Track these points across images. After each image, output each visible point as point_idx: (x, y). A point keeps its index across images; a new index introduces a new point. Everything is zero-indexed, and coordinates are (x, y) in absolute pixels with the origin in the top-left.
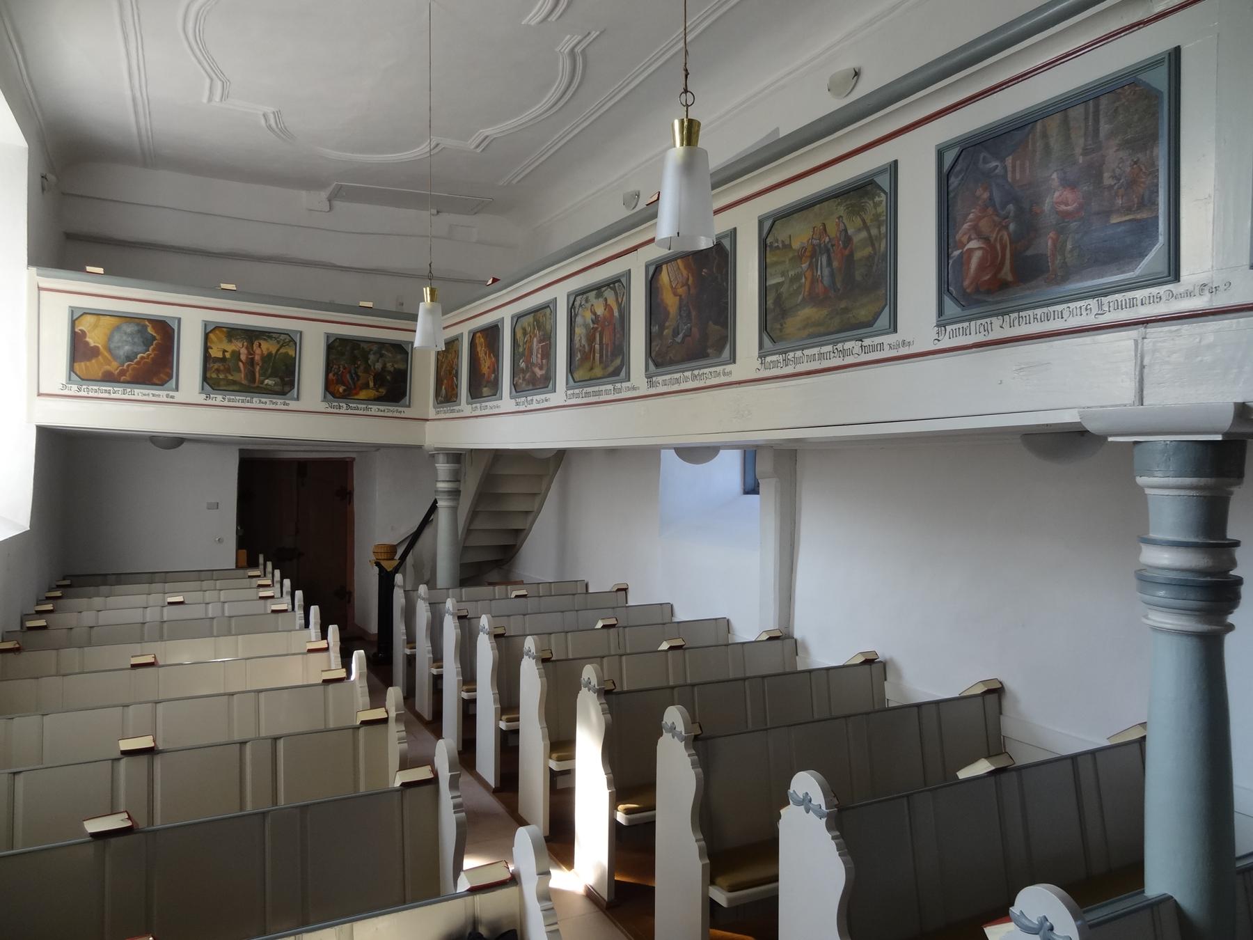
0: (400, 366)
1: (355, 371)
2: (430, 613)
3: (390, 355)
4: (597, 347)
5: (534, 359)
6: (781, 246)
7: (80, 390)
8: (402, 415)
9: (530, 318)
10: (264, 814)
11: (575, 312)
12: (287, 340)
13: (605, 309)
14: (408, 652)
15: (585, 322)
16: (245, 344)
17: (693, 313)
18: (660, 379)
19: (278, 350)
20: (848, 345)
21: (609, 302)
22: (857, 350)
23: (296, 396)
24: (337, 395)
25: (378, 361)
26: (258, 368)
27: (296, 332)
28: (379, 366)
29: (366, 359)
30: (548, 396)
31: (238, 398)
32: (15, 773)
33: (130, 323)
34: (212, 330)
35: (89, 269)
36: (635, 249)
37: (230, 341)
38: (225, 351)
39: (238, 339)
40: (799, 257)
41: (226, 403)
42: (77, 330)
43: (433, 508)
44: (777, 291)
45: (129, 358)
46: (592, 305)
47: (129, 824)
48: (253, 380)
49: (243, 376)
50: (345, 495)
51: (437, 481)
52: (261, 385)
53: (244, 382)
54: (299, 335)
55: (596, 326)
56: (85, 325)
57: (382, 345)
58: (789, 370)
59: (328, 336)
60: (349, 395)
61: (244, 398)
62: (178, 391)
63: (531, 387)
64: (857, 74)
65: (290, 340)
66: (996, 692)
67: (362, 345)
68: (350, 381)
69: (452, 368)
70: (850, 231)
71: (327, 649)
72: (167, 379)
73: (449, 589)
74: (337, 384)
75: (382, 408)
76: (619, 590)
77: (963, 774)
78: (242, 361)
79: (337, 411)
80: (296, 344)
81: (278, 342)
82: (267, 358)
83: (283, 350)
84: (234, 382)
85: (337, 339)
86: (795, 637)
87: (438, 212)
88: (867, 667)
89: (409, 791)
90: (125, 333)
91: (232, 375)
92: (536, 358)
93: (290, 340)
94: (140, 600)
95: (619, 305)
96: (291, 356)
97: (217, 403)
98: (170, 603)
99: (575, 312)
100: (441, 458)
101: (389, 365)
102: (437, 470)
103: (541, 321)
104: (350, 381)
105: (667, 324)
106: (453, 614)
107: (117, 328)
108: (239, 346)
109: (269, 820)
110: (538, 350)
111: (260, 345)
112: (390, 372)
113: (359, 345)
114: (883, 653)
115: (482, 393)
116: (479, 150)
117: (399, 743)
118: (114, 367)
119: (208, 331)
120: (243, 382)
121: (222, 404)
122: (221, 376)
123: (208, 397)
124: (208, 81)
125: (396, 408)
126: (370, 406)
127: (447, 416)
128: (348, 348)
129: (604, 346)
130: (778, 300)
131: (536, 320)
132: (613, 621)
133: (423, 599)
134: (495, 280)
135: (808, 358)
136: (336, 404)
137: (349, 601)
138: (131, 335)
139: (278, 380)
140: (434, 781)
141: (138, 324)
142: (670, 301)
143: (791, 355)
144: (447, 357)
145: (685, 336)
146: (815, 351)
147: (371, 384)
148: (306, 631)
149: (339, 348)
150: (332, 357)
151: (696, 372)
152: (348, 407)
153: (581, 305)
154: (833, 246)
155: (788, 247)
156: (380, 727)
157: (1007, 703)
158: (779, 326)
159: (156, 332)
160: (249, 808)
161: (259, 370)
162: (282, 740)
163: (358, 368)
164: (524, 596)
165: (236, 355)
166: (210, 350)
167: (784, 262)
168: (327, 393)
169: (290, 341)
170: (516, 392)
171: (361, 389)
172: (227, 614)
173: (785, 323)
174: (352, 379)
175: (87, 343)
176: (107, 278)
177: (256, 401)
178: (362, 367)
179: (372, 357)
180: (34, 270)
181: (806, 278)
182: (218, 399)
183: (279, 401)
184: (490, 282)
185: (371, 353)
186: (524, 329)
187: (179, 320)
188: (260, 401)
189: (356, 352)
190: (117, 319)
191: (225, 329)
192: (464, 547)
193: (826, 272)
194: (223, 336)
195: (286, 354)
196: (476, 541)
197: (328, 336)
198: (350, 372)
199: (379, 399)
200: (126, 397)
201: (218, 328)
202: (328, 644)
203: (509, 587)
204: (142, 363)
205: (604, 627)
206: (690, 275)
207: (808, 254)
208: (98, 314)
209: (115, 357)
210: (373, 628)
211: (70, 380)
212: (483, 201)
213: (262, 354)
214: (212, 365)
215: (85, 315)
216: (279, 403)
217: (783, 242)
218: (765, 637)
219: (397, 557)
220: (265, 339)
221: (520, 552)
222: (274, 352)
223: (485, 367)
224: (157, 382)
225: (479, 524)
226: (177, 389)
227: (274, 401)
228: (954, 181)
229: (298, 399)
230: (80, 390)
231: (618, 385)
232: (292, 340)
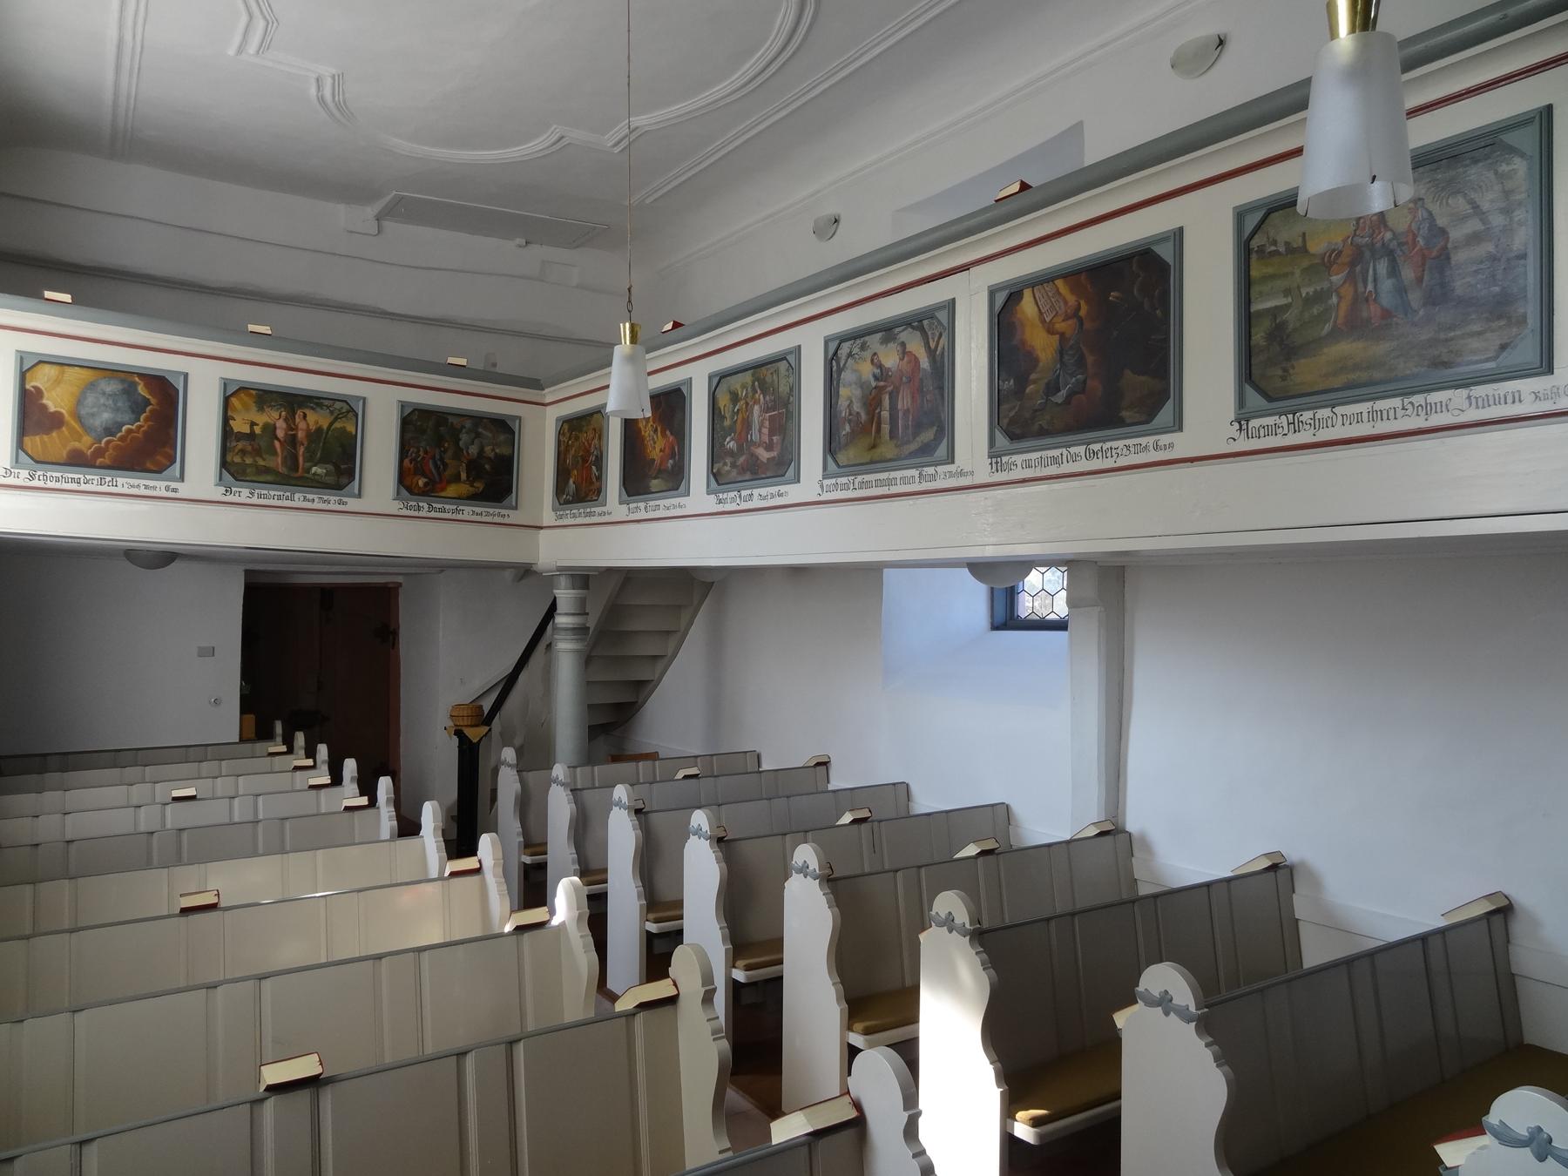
0: (504, 451)
1: (441, 456)
3: (490, 435)
4: (885, 414)
5: (755, 437)
6: (1282, 249)
7: (32, 477)
8: (506, 521)
9: (747, 377)
11: (838, 364)
12: (344, 411)
13: (902, 359)
15: (860, 378)
16: (283, 413)
17: (1090, 359)
18: (1018, 459)
19: (331, 424)
21: (909, 348)
23: (356, 491)
25: (473, 443)
26: (301, 450)
27: (358, 398)
28: (473, 450)
30: (783, 488)
31: (272, 493)
32: (82, 1143)
33: (110, 378)
35: (48, 294)
36: (965, 268)
37: (261, 409)
38: (253, 424)
39: (271, 406)
41: (255, 500)
42: (28, 387)
44: (1275, 318)
45: (109, 431)
46: (875, 354)
48: (295, 467)
50: (387, 635)
52: (306, 475)
54: (361, 403)
55: (882, 384)
57: (478, 420)
59: (403, 405)
60: (433, 490)
61: (282, 493)
62: (183, 481)
63: (747, 477)
64: (1221, 42)
65: (348, 409)
66: (1503, 912)
67: (451, 419)
68: (433, 470)
69: (588, 452)
72: (168, 464)
74: (415, 474)
75: (478, 510)
76: (818, 764)
78: (279, 441)
79: (416, 514)
81: (332, 412)
82: (316, 435)
83: (337, 425)
84: (267, 470)
85: (415, 410)
86: (1132, 826)
88: (1272, 874)
90: (104, 393)
91: (264, 460)
92: (759, 431)
93: (348, 409)
95: (931, 353)
96: (351, 433)
97: (242, 500)
99: (838, 364)
100: (563, 581)
101: (488, 449)
103: (768, 379)
104: (433, 470)
105: (1033, 376)
107: (91, 386)
108: (273, 416)
110: (761, 425)
111: (305, 416)
112: (490, 458)
114: (1292, 855)
115: (648, 487)
116: (617, 150)
117: (714, 1040)
118: (85, 443)
119: (228, 394)
120: (280, 470)
122: (249, 461)
123: (228, 491)
124: (244, 19)
125: (497, 511)
126: (461, 508)
127: (579, 521)
129: (900, 414)
130: (1278, 333)
131: (756, 378)
134: (676, 325)
136: (414, 503)
138: (112, 396)
139: (330, 467)
141: (123, 381)
144: (577, 438)
146: (1364, 407)
147: (464, 476)
149: (419, 423)
151: (1096, 447)
153: (850, 355)
154: (1400, 244)
156: (665, 1011)
157: (1518, 928)
158: (1280, 372)
159: (150, 394)
161: (304, 452)
162: (521, 1044)
163: (445, 452)
164: (695, 776)
165: (270, 429)
166: (231, 422)
167: (1293, 274)
169: (348, 412)
170: (719, 484)
171: (449, 482)
173: (1293, 367)
175: (45, 407)
176: (76, 309)
177: (299, 499)
178: (450, 453)
179: (464, 437)
181: (1340, 298)
182: (243, 494)
184: (669, 326)
185: (464, 431)
187: (186, 376)
188: (305, 497)
189: (442, 428)
191: (254, 392)
193: (1387, 285)
194: (250, 402)
195: (343, 430)
197: (403, 405)
198: (433, 458)
199: (475, 498)
200: (104, 489)
201: (244, 389)
202: (480, 861)
204: (130, 437)
205: (855, 821)
206: (1082, 303)
207: (1344, 259)
209: (87, 429)
211: (17, 462)
212: (595, 228)
214: (234, 444)
215: (40, 366)
216: (333, 501)
217: (1287, 244)
218: (1093, 831)
220: (313, 409)
222: (325, 427)
226: (182, 478)
227: (325, 498)
229: (359, 496)
230: (32, 477)
231: (930, 470)
232: (352, 410)
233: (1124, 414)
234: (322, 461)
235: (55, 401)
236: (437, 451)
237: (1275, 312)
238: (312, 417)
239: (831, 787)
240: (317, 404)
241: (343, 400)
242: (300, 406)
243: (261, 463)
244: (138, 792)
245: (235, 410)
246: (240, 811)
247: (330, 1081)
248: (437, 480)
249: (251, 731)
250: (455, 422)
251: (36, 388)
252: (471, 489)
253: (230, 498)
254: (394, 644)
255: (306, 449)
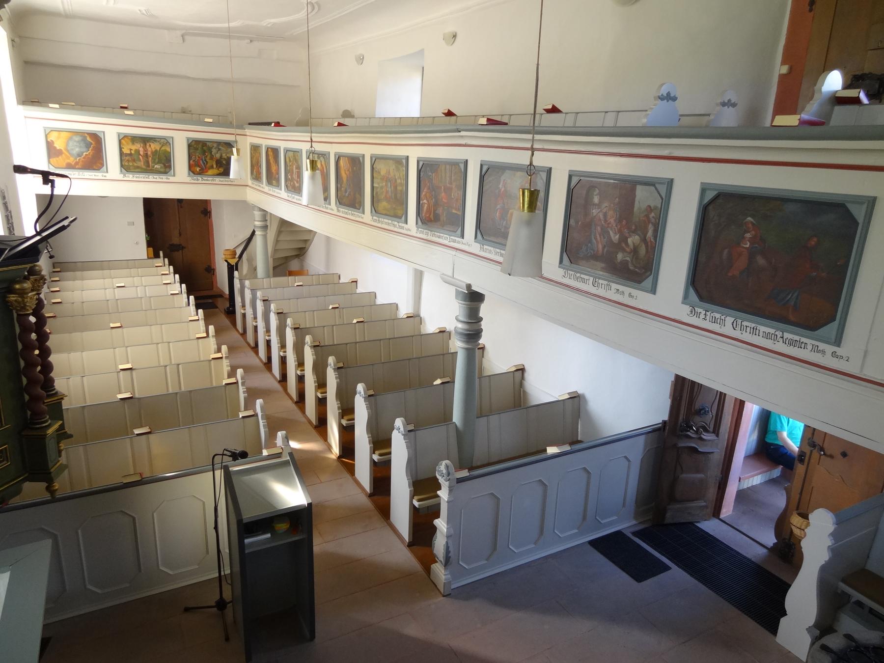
2: (251, 295)
3: (224, 149)
10: (177, 393)
14: (243, 312)
17: (351, 185)
18: (341, 209)
19: (160, 148)
20: (396, 223)
22: (397, 226)
23: (173, 174)
24: (196, 173)
25: (217, 153)
26: (150, 159)
28: (218, 156)
29: (211, 152)
31: (141, 176)
34: (123, 137)
35: (51, 105)
38: (131, 150)
40: (382, 179)
41: (135, 179)
42: (49, 140)
43: (253, 233)
45: (79, 155)
47: (132, 396)
48: (148, 166)
49: (142, 163)
51: (255, 221)
53: (144, 167)
54: (171, 139)
56: (53, 137)
57: (219, 143)
58: (379, 225)
59: (188, 139)
60: (203, 173)
64: (455, 36)
65: (166, 142)
67: (208, 143)
70: (396, 177)
71: (198, 320)
73: (263, 278)
74: (195, 166)
75: (221, 179)
76: (352, 282)
77: (435, 383)
78: (140, 155)
79: (196, 182)
80: (170, 144)
81: (160, 144)
82: (155, 153)
83: (163, 148)
84: (138, 167)
86: (422, 315)
87: (251, 41)
88: (441, 334)
89: (227, 386)
90: (75, 141)
91: (136, 163)
94: (99, 282)
96: (168, 151)
98: (118, 287)
100: (256, 209)
101: (224, 155)
102: (254, 214)
106: (260, 300)
107: (70, 138)
108: (138, 146)
109: (178, 396)
111: (150, 146)
112: (225, 159)
113: (206, 144)
118: (71, 160)
119: (120, 138)
121: (133, 179)
122: (131, 164)
123: (124, 176)
127: (257, 187)
128: (200, 146)
130: (377, 193)
131: (294, 156)
132: (337, 306)
133: (247, 288)
135: (386, 223)
137: (214, 274)
138: (78, 142)
140: (237, 383)
141: (81, 136)
142: (344, 175)
143: (380, 219)
145: (349, 194)
146: (386, 221)
147: (215, 166)
148: (188, 308)
150: (191, 151)
151: (353, 212)
152: (203, 179)
155: (379, 173)
159: (92, 140)
160: (171, 391)
163: (206, 157)
165: (137, 151)
166: (123, 149)
168: (191, 173)
169: (167, 143)
171: (209, 169)
172: (148, 296)
174: (204, 164)
177: (151, 178)
178: (209, 157)
179: (214, 151)
180: (21, 107)
182: (130, 177)
183: (164, 177)
186: (289, 158)
187: (104, 132)
190: (69, 133)
191: (130, 137)
192: (275, 250)
193: (390, 190)
195: (165, 150)
196: (282, 246)
197: (188, 139)
198: (202, 160)
199: (219, 175)
201: (126, 136)
203: (296, 277)
205: (332, 308)
208: (59, 131)
210: (227, 291)
213: (152, 151)
214: (124, 158)
215: (52, 132)
216: (164, 178)
219: (237, 256)
220: (152, 142)
221: (309, 250)
222: (158, 149)
223: (274, 168)
224: (97, 168)
225: (282, 238)
226: (107, 172)
227: (161, 177)
228: (422, 174)
229: (174, 176)
233: (357, 205)
234: (158, 163)
235: (59, 145)
236: (203, 157)
237: (377, 187)
238: (153, 146)
239: (358, 291)
240: (155, 141)
241: (164, 138)
242: (148, 142)
243: (135, 165)
244: (108, 281)
245: (123, 145)
246: (140, 292)
247: (134, 369)
248: (204, 168)
249: (152, 255)
250: (210, 145)
251: (52, 141)
252: (219, 171)
253: (125, 179)
254: (210, 218)
255: (152, 158)
